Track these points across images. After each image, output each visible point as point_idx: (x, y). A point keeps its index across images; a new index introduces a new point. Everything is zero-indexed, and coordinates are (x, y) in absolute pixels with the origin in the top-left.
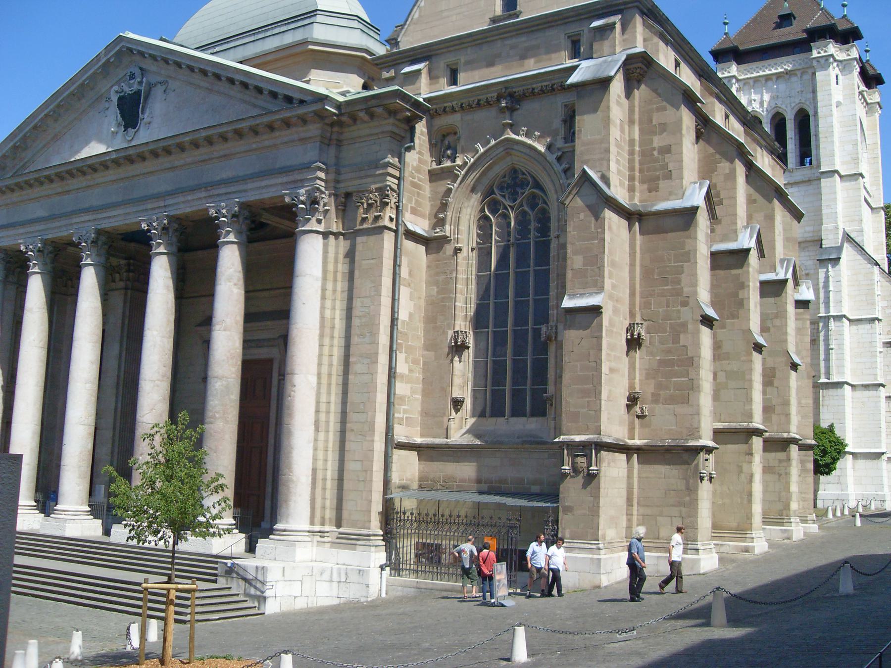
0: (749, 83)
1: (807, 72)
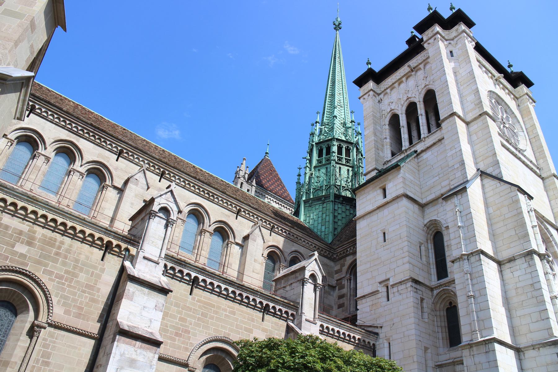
0: (387, 93)
1: (428, 62)
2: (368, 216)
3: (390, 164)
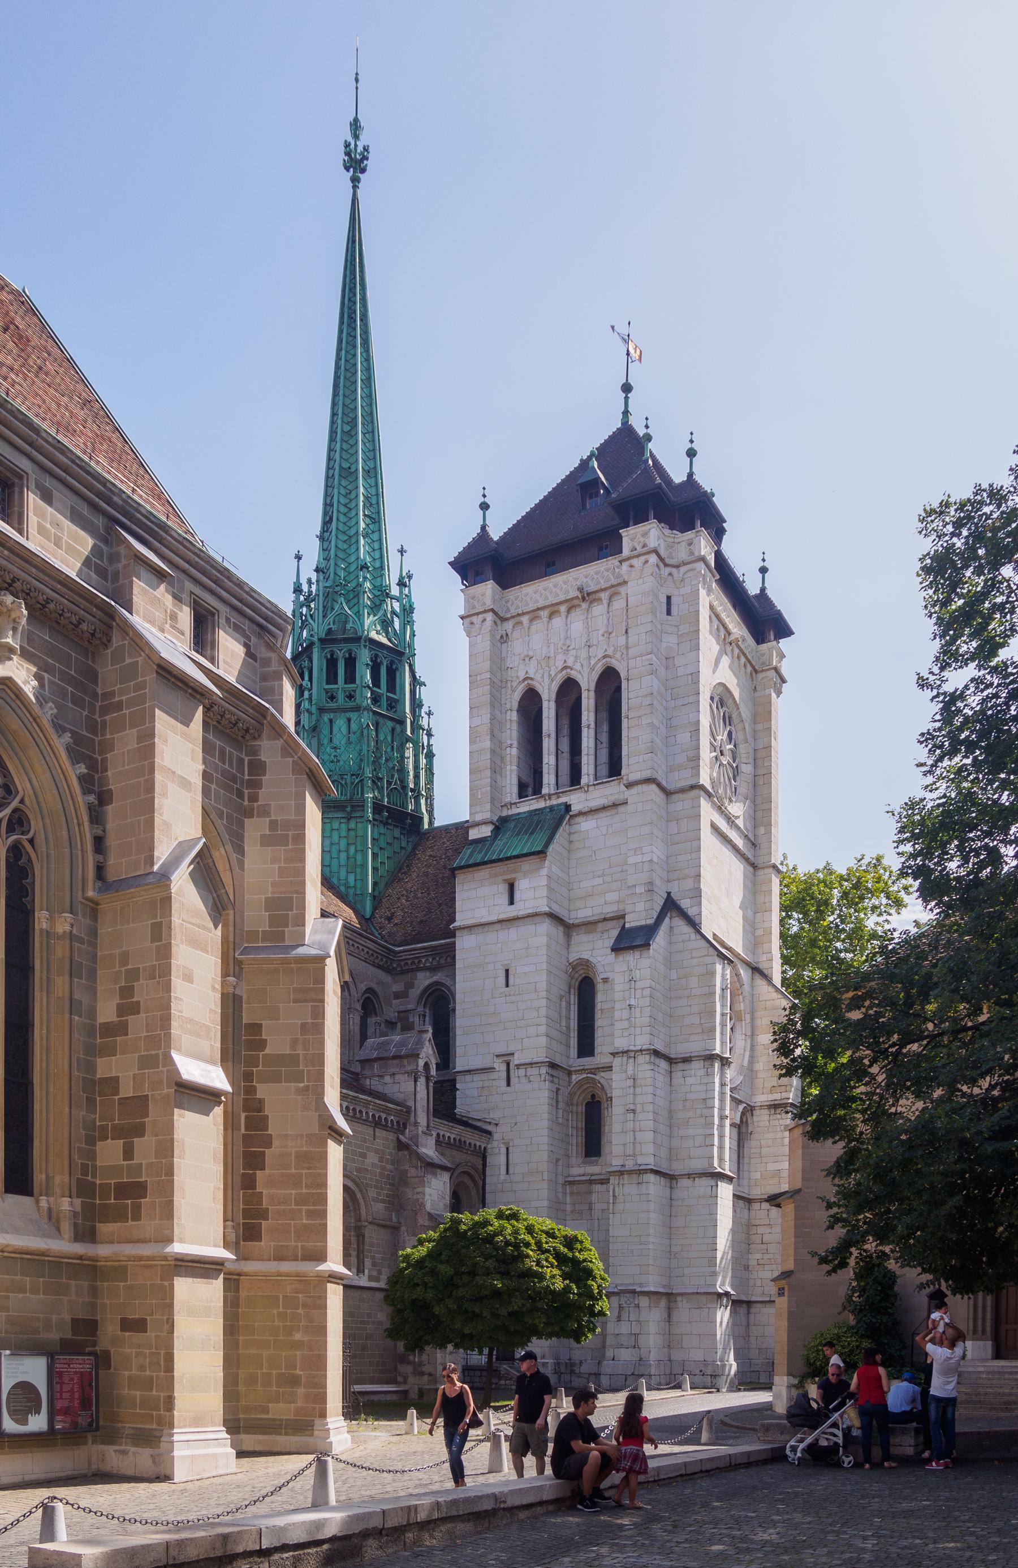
2: (480, 928)
3: (515, 811)
